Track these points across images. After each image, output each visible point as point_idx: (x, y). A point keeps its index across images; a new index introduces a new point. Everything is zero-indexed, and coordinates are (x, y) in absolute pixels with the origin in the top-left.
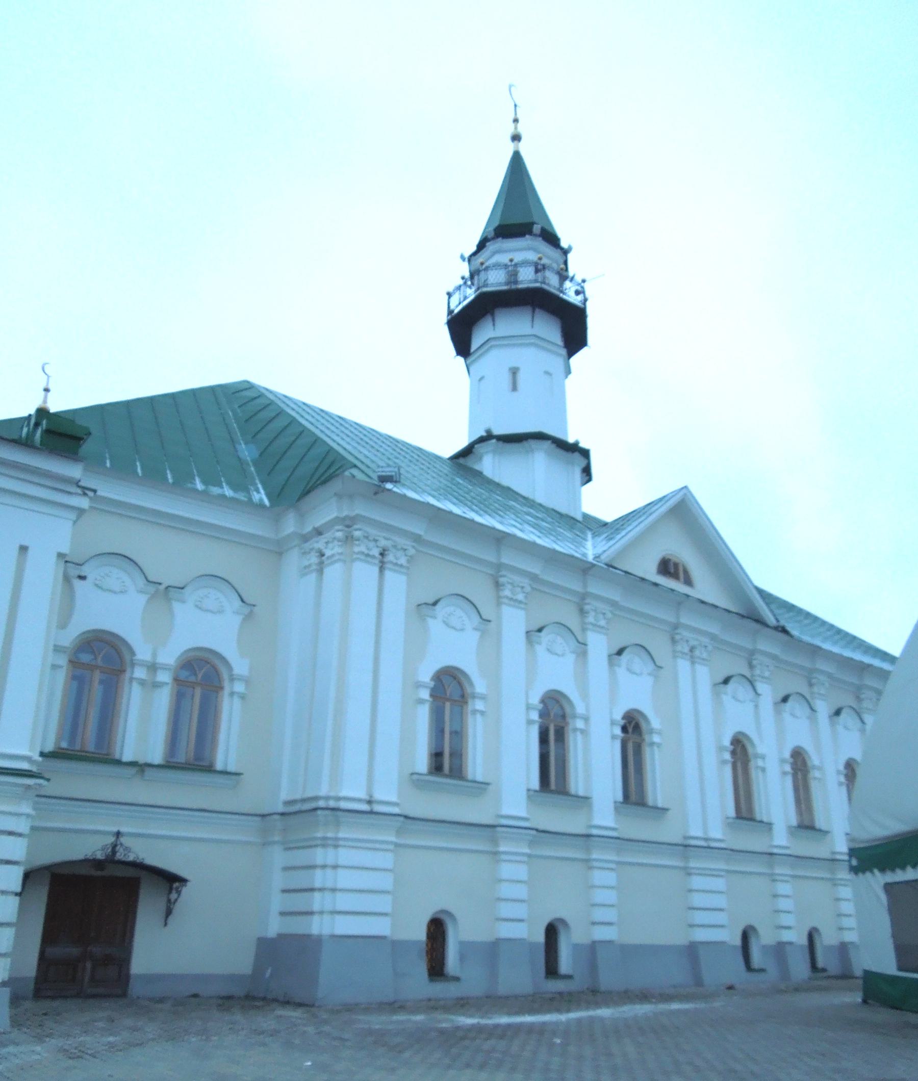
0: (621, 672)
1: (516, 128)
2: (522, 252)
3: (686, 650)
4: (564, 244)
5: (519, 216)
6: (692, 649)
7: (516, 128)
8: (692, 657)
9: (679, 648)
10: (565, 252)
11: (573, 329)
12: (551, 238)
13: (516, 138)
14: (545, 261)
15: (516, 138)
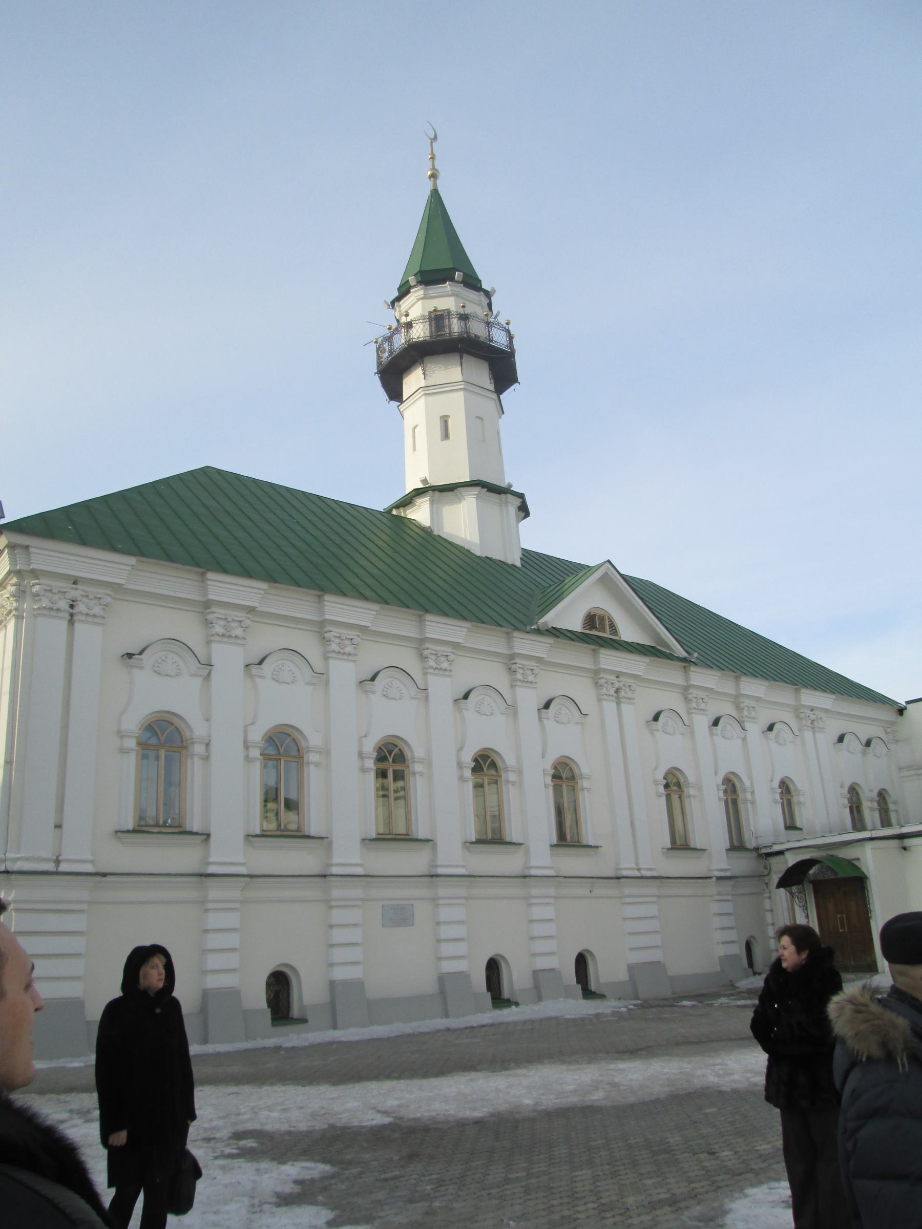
0: (549, 724)
1: (433, 165)
2: (447, 299)
3: (612, 692)
4: (485, 286)
5: (441, 259)
6: (617, 691)
7: (433, 165)
8: (617, 698)
9: (605, 691)
10: (488, 294)
11: (502, 369)
12: (472, 282)
13: (434, 176)
14: (467, 311)
15: (434, 176)
